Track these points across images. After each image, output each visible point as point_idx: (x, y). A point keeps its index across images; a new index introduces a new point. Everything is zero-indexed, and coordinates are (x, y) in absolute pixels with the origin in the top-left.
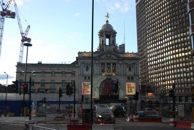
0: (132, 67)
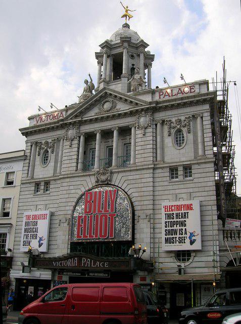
0: (184, 130)
